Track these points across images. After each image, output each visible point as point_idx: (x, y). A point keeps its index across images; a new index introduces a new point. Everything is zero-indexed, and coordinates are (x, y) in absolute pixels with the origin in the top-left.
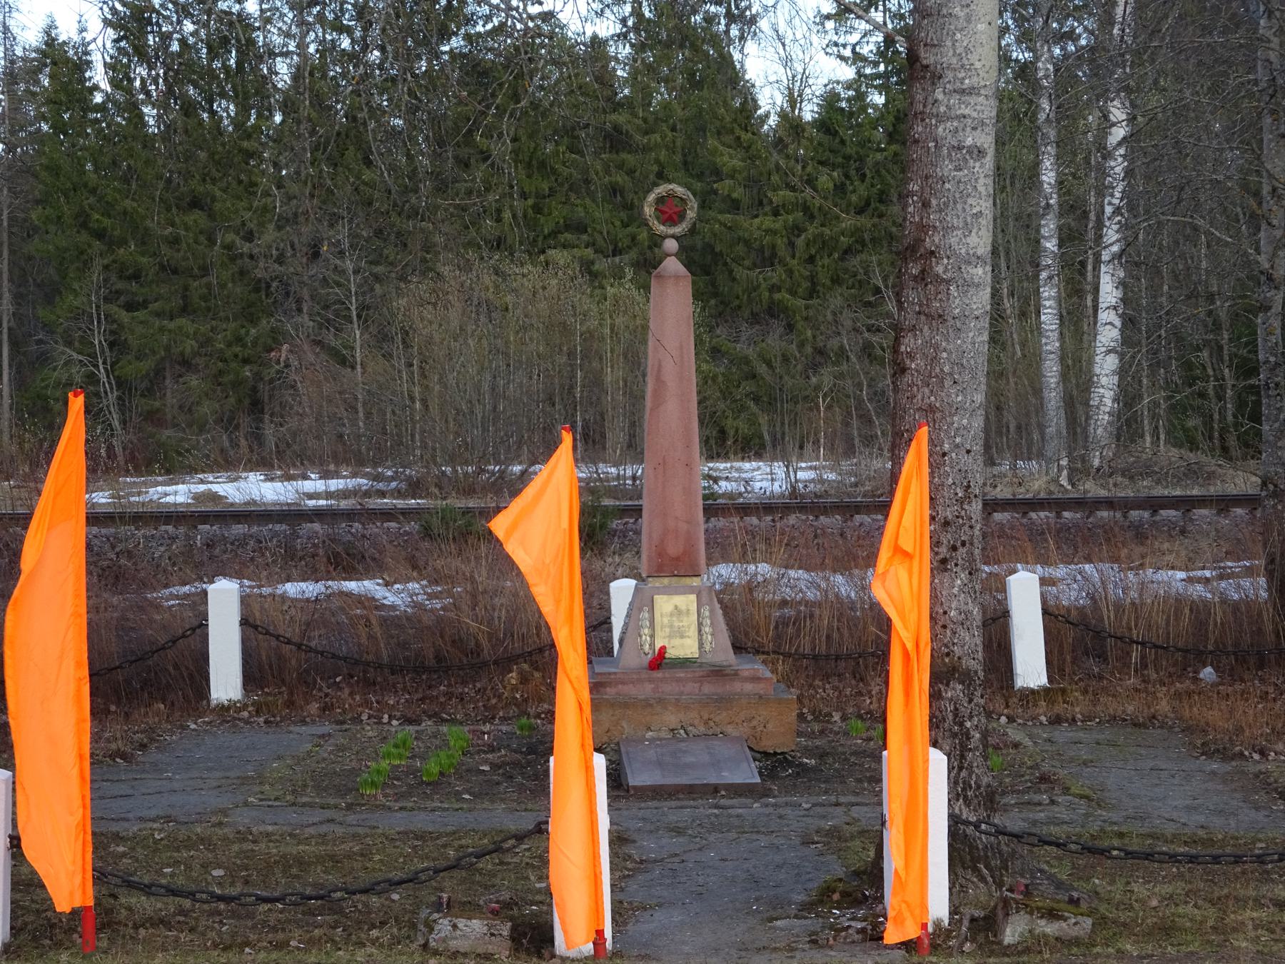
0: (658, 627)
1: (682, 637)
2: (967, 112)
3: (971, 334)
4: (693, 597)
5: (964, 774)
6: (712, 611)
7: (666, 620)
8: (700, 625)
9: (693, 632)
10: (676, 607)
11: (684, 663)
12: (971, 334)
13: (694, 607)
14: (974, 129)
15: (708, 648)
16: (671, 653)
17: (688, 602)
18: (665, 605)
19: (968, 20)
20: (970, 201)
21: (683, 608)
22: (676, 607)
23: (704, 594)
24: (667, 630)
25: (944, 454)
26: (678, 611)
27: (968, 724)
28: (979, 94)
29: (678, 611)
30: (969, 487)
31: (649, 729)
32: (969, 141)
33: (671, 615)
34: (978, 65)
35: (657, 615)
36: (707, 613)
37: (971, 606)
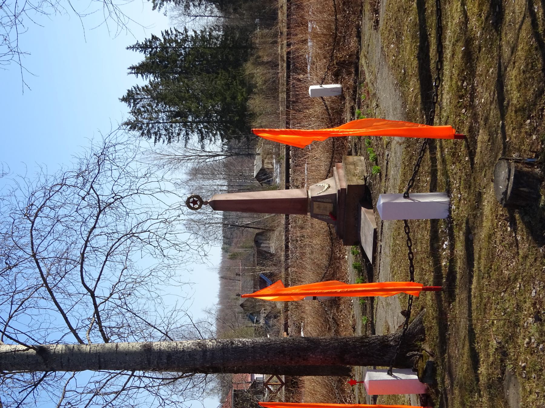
1: (326, 207)
2: (155, 362)
3: (229, 355)
5: (375, 356)
9: (326, 204)
11: (334, 207)
12: (229, 355)
14: (161, 359)
15: (330, 201)
16: (332, 209)
18: (316, 211)
19: (126, 363)
20: (185, 359)
25: (269, 361)
26: (319, 207)
27: (358, 353)
28: (150, 358)
29: (319, 207)
30: (279, 352)
32: (165, 361)
34: (140, 359)
35: (319, 213)
37: (319, 350)
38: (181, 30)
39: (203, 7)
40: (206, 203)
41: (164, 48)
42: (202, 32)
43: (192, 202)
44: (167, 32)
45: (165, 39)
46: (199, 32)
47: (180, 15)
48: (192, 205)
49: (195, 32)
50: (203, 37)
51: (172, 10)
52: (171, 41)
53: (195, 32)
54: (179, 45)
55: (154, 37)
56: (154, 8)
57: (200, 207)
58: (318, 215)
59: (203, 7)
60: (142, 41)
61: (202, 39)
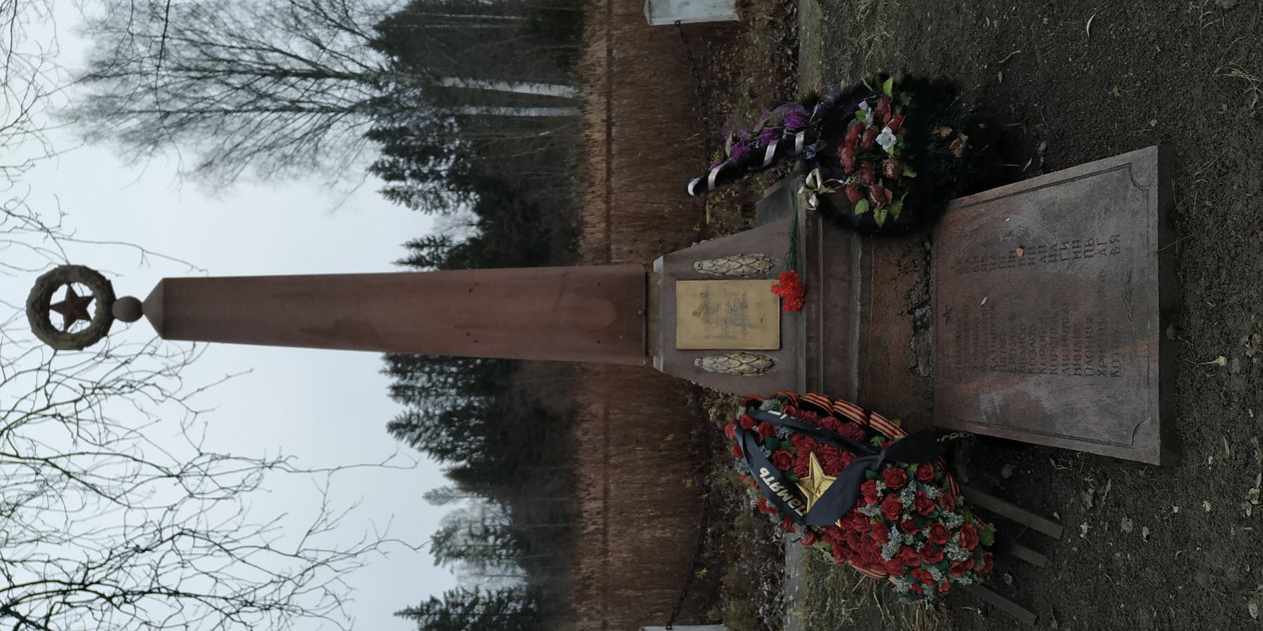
0: (728, 344)
1: (744, 305)
4: (681, 286)
6: (704, 256)
7: (717, 330)
8: (724, 277)
10: (695, 314)
13: (699, 286)
17: (688, 295)
21: (699, 302)
22: (695, 314)
23: (676, 268)
24: (731, 329)
29: (706, 311)
31: (913, 369)
33: (707, 321)
36: (707, 265)
38: (471, 590)
39: (503, 566)
40: (133, 310)
41: (445, 614)
42: (499, 593)
43: (59, 308)
44: (452, 595)
45: (447, 602)
46: (494, 593)
47: (471, 575)
48: (57, 319)
49: (489, 593)
50: (500, 601)
51: (462, 568)
52: (455, 605)
53: (489, 593)
54: (468, 610)
55: (434, 601)
56: (437, 563)
57: (101, 330)
58: (702, 353)
59: (503, 566)
60: (415, 605)
61: (497, 605)
